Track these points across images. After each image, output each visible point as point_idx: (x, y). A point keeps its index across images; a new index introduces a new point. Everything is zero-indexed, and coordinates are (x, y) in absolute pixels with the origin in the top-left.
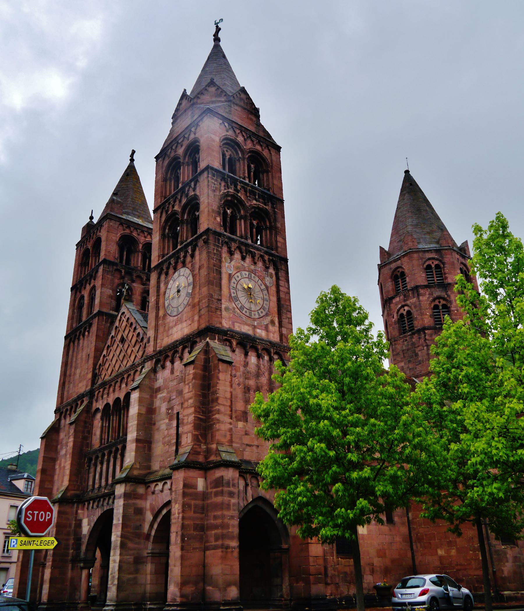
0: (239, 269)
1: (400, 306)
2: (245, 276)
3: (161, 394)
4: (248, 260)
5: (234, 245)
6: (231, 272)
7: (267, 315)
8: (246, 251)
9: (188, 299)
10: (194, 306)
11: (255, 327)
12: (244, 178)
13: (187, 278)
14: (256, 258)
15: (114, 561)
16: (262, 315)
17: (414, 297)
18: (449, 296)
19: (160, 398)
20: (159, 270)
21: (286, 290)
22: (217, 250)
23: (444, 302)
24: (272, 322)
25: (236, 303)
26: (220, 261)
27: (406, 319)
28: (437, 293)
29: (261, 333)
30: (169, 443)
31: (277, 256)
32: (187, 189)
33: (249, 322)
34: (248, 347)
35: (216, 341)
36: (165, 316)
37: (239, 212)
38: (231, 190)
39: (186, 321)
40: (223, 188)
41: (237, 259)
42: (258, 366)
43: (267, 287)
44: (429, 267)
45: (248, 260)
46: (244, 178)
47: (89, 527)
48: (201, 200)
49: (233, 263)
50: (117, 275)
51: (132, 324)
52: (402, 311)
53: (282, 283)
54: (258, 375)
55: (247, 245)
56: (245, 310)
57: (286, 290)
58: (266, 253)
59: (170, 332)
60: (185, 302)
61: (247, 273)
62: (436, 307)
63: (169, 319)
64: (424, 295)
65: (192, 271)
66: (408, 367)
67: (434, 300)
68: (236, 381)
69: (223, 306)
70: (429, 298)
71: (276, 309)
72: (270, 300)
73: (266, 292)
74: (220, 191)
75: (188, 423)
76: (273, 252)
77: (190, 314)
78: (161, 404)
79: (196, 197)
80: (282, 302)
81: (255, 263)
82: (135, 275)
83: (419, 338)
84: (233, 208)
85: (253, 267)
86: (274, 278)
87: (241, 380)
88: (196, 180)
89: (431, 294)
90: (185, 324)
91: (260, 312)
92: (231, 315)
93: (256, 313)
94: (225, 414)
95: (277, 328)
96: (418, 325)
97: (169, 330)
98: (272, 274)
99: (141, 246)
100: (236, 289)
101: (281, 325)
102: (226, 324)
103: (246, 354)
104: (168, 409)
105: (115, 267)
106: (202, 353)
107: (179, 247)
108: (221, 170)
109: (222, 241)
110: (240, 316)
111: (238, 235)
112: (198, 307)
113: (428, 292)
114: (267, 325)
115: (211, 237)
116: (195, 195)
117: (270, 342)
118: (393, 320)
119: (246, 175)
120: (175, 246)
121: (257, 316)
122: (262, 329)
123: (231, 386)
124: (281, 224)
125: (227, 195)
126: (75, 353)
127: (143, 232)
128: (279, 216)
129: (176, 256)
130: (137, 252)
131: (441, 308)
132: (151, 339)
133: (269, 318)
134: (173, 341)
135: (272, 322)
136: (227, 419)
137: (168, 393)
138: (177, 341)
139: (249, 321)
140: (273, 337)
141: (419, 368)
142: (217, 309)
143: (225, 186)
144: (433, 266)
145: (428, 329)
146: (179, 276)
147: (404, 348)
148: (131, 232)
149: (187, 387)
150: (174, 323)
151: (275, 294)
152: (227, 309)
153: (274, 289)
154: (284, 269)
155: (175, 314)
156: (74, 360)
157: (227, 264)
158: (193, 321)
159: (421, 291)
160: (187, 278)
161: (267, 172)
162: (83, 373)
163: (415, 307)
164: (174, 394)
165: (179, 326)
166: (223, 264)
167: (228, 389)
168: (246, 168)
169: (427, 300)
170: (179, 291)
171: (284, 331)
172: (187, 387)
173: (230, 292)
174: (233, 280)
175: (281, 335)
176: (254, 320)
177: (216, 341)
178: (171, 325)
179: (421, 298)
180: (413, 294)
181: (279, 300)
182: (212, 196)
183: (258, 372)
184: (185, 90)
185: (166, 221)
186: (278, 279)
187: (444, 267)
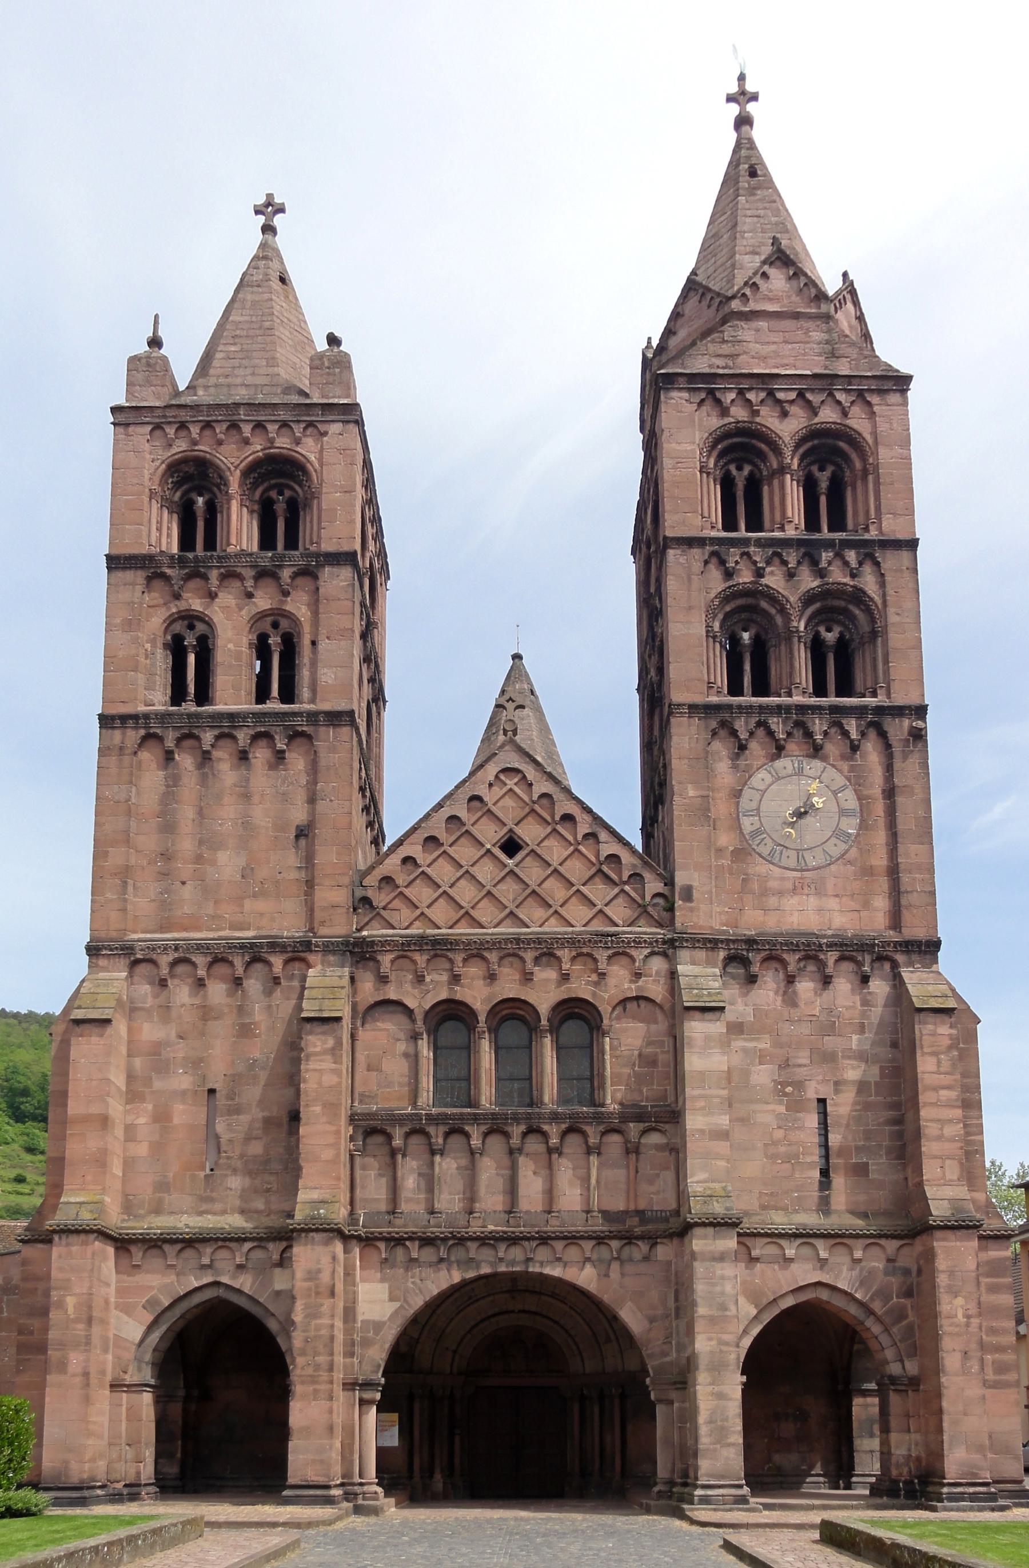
3: (745, 1040)
13: (835, 793)
19: (745, 1050)
30: (792, 1159)
36: (742, 853)
39: (837, 896)
47: (397, 1304)
59: (773, 901)
90: (833, 903)
112: (883, 883)
132: (695, 894)
134: (784, 928)
137: (777, 1044)
150: (789, 885)
155: (792, 863)
158: (866, 905)
170: (800, 815)
185: (727, 597)
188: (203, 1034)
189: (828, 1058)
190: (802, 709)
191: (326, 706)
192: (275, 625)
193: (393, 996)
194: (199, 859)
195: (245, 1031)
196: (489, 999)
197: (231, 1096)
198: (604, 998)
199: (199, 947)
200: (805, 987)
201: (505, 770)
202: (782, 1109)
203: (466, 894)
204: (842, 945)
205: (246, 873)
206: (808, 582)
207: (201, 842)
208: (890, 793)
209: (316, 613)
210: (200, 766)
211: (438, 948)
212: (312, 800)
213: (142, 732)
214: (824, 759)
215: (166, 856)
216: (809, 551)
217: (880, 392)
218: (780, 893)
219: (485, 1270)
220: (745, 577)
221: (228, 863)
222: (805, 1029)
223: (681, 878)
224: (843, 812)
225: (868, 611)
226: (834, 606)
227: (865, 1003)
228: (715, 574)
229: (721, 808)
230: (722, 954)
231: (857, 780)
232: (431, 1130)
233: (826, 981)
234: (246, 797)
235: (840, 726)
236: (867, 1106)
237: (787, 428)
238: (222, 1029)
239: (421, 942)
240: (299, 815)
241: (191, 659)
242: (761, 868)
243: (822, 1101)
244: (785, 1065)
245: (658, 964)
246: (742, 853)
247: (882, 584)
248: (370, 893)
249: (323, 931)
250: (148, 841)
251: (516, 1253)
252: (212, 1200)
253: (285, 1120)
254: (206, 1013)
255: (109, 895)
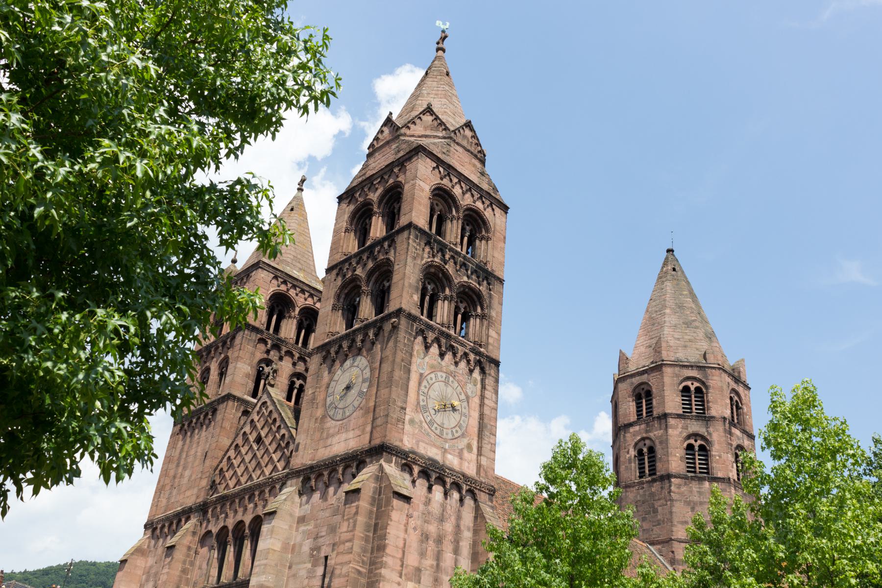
0: (434, 369)
1: (639, 438)
2: (440, 379)
4: (449, 356)
5: (431, 336)
6: (422, 372)
7: (463, 436)
8: (446, 345)
9: (360, 400)
10: (367, 412)
11: (445, 451)
12: (455, 245)
13: (362, 371)
14: (459, 355)
16: (456, 435)
17: (661, 429)
18: (710, 434)
19: (304, 532)
20: (324, 353)
21: (492, 404)
22: (409, 339)
23: (703, 443)
24: (469, 447)
25: (425, 415)
26: (411, 355)
27: (646, 458)
28: (695, 427)
29: (452, 461)
31: (487, 357)
32: (377, 249)
33: (438, 444)
34: (434, 477)
35: (393, 465)
37: (444, 291)
38: (437, 259)
40: (426, 255)
41: (434, 354)
42: (443, 507)
43: (468, 397)
44: (686, 389)
45: (449, 356)
46: (455, 245)
48: (396, 267)
49: (427, 359)
50: (261, 347)
51: (275, 420)
52: (641, 445)
53: (488, 394)
54: (442, 519)
55: (448, 336)
56: (435, 425)
57: (492, 404)
58: (473, 350)
59: (329, 441)
60: (356, 404)
61: (444, 375)
62: (690, 447)
63: (330, 423)
64: (676, 427)
65: (371, 363)
66: (641, 527)
67: (689, 437)
68: (412, 523)
69: (407, 418)
70: (681, 433)
71: (476, 430)
72: (470, 416)
73: (465, 404)
74: (422, 259)
75: (340, 576)
76: (482, 350)
77: (361, 421)
78: (304, 540)
79: (388, 264)
80: (486, 421)
81: (456, 364)
82: (284, 349)
83: (662, 488)
84: (435, 284)
85: (452, 367)
86: (479, 386)
87: (419, 523)
88: (390, 238)
89: (685, 428)
90: (351, 434)
91: (454, 430)
92: (416, 431)
93: (450, 431)
94: (393, 570)
95: (473, 456)
96: (661, 469)
97: (327, 438)
98: (476, 379)
99: (297, 310)
100: (426, 395)
101: (480, 454)
102: (407, 443)
103: (430, 488)
104: (312, 549)
105: (259, 336)
106: (372, 480)
107: (356, 326)
108: (426, 229)
109: (417, 328)
110: (428, 434)
111: (438, 321)
112: (371, 415)
113: (680, 423)
114: (462, 450)
115: (403, 321)
116: (388, 259)
117: (464, 475)
118: (628, 456)
119: (459, 240)
120: (349, 325)
121: (450, 436)
122: (454, 455)
123: (406, 531)
124: (497, 313)
125: (429, 266)
126: (186, 447)
127: (303, 291)
128: (495, 302)
129: (350, 337)
130: (290, 317)
131: (697, 448)
132: (300, 447)
133: (465, 441)
134: (331, 455)
135: (469, 447)
136: (395, 577)
137: (316, 526)
138: (337, 456)
139: (439, 442)
140: (468, 468)
141: (656, 530)
142: (398, 421)
143: (429, 253)
144: (692, 388)
145: (675, 477)
146: (352, 366)
147: (639, 498)
148: (288, 290)
149: (346, 524)
150: (337, 430)
151: (477, 408)
152: (412, 421)
153: (476, 401)
154: (493, 374)
156: (184, 456)
157: (419, 360)
158: (364, 430)
159: (672, 421)
160: (362, 371)
161: (488, 239)
162: (193, 478)
164: (325, 529)
165: (344, 436)
166: (414, 360)
167: (402, 535)
168: (459, 231)
169: (679, 436)
170: (348, 388)
171: (484, 461)
172: (346, 524)
173: (418, 399)
174: (425, 383)
175: (479, 467)
176: (446, 441)
177: (393, 465)
178: (331, 431)
179: (670, 431)
180: (660, 424)
181: (482, 416)
182: (412, 265)
183: (443, 515)
184: (391, 113)
185: (342, 287)
186: (483, 387)
187: (707, 393)
202: (309, 566)
204: (345, 458)
206: (370, 265)
218: (333, 436)
222: (327, 514)
224: (364, 381)
243: (326, 558)
244: (317, 538)
246: (324, 417)
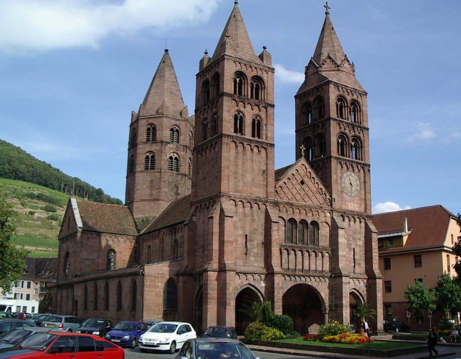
15: (347, 313)
17: (183, 152)
36: (342, 192)
59: (347, 203)
90: (356, 205)
112: (363, 202)
147: (170, 180)
158: (361, 206)
163: (183, 158)
164: (351, 238)
188: (244, 220)
189: (355, 239)
190: (352, 161)
191: (269, 142)
192: (256, 117)
193: (282, 216)
194: (243, 175)
195: (253, 221)
196: (299, 218)
197: (250, 237)
198: (319, 222)
199: (245, 198)
200: (352, 223)
201: (302, 164)
202: (348, 250)
203: (294, 192)
205: (253, 180)
207: (243, 171)
208: (365, 182)
209: (267, 118)
210: (243, 151)
211: (291, 205)
212: (267, 164)
213: (232, 140)
214: (354, 173)
215: (236, 173)
216: (353, 126)
217: (363, 95)
219: (298, 283)
220: (343, 130)
221: (249, 178)
222: (351, 232)
223: (334, 196)
224: (357, 185)
225: (361, 141)
226: (356, 139)
227: (360, 228)
228: (338, 127)
229: (339, 181)
230: (340, 214)
231: (359, 178)
232: (289, 249)
233: (355, 222)
234: (252, 161)
235: (357, 166)
236: (360, 250)
237: (349, 98)
238: (248, 219)
239: (288, 203)
240: (264, 168)
241: (238, 122)
242: (345, 195)
243: (354, 249)
244: (348, 240)
245: (328, 215)
247: (364, 137)
248: (277, 190)
249: (270, 198)
250: (232, 168)
251: (303, 279)
252: (246, 263)
253: (261, 244)
254: (245, 215)
255: (225, 182)
